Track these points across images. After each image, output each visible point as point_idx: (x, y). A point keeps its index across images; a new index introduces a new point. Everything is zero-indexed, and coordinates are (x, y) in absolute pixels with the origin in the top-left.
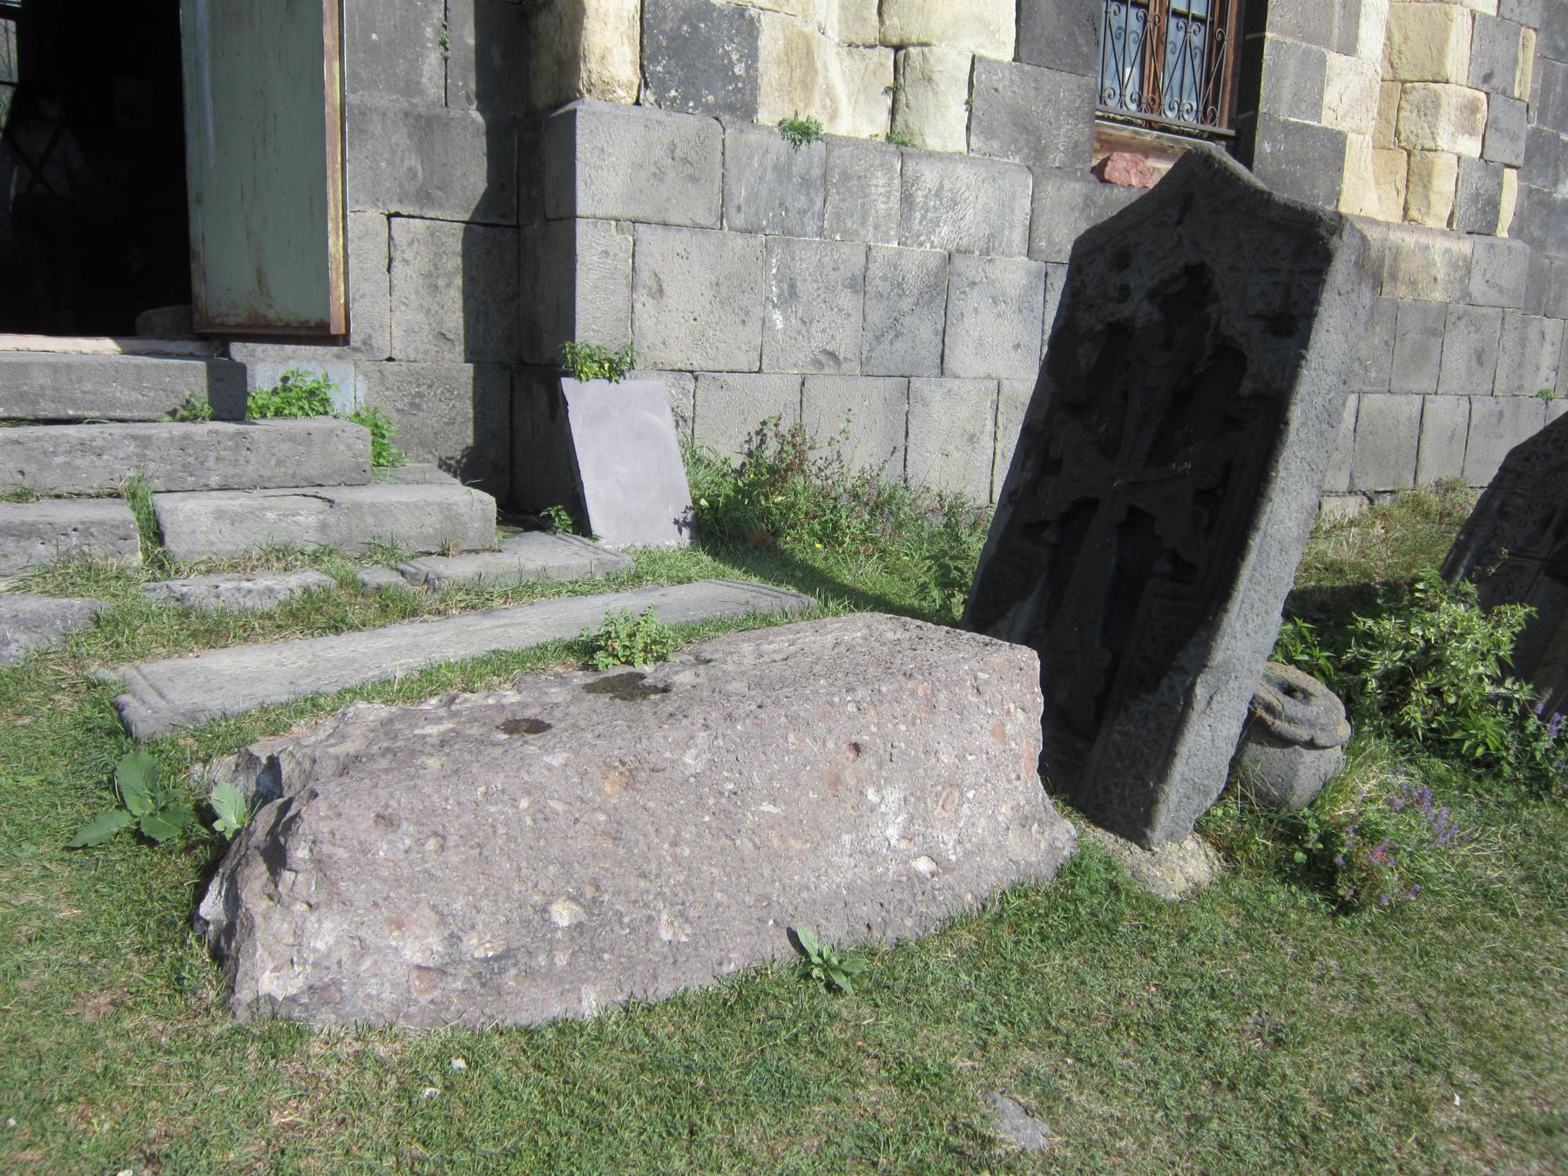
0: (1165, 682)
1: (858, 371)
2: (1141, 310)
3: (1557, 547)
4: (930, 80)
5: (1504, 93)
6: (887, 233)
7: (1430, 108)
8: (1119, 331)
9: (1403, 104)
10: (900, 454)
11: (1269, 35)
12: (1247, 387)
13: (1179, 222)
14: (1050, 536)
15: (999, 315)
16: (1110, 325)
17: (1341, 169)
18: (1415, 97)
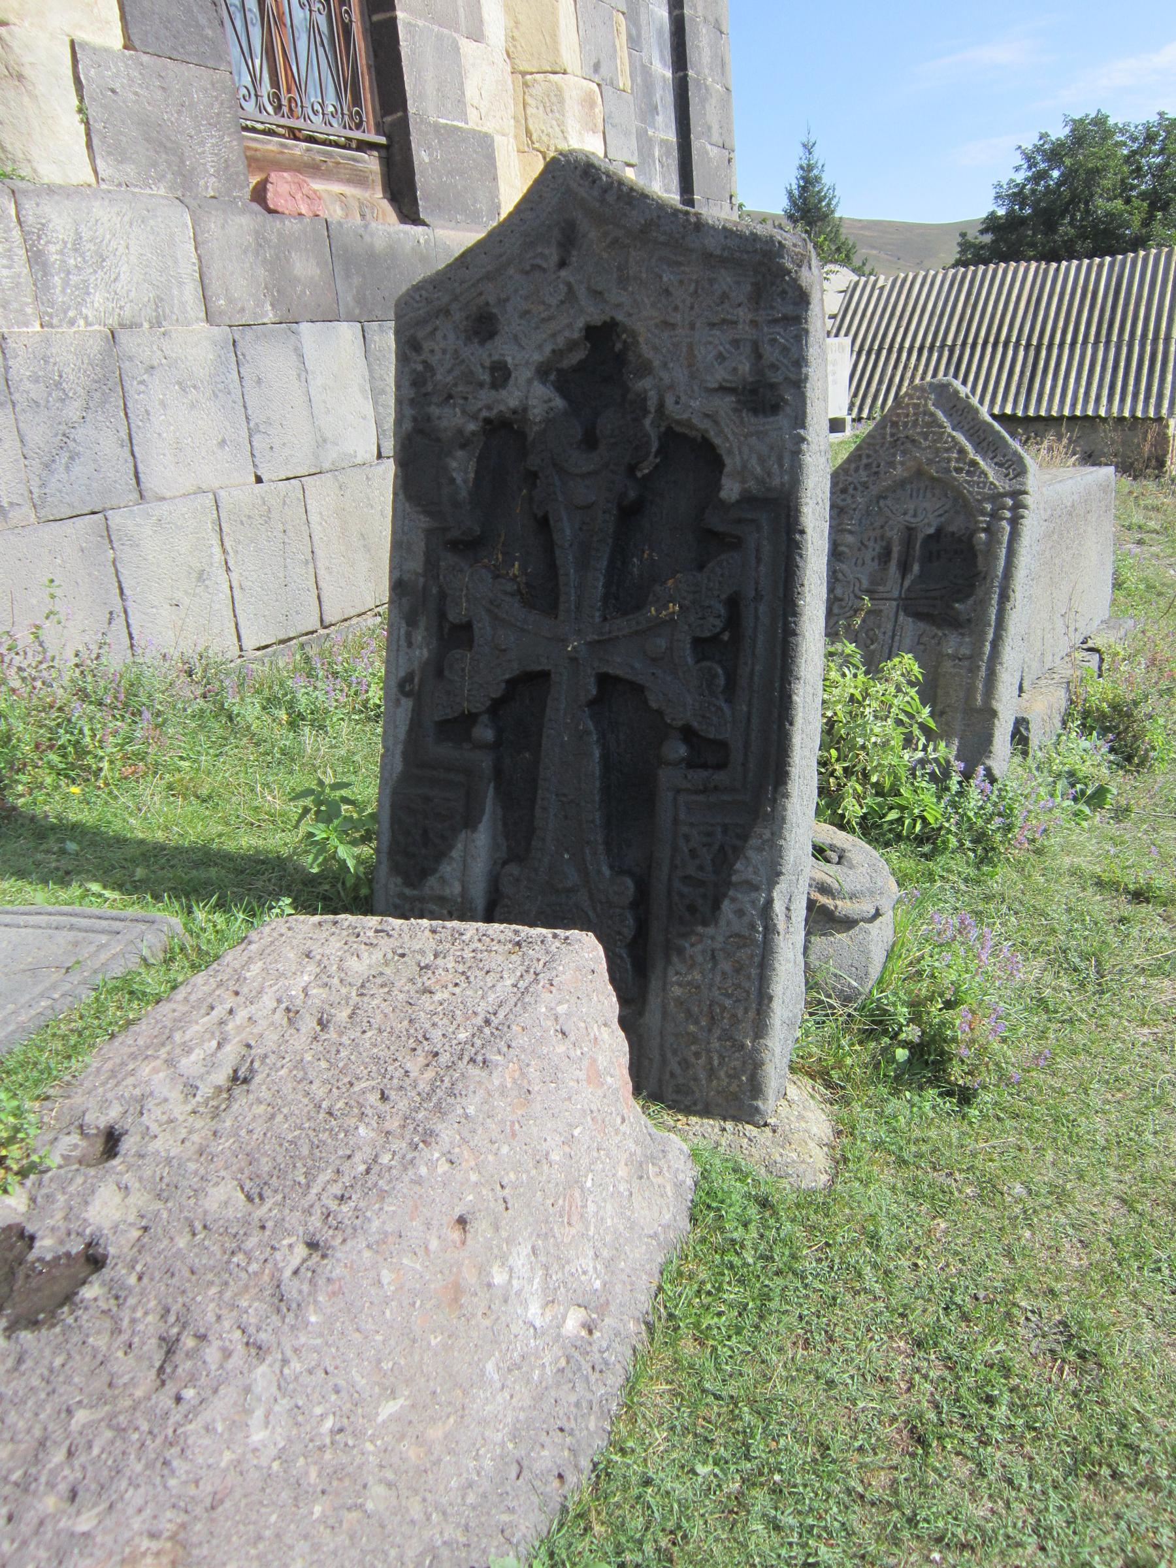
0: (726, 905)
1: (33, 519)
2: (531, 397)
3: (907, 583)
4: (20, 77)
5: (612, 84)
6: (21, 311)
7: (555, 102)
8: (503, 430)
9: (529, 100)
10: (120, 621)
11: (400, 15)
12: (730, 490)
13: (562, 264)
14: (485, 732)
15: (193, 406)
16: (487, 421)
17: (495, 179)
18: (537, 90)
